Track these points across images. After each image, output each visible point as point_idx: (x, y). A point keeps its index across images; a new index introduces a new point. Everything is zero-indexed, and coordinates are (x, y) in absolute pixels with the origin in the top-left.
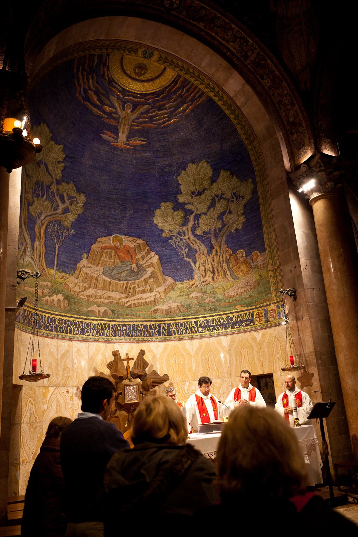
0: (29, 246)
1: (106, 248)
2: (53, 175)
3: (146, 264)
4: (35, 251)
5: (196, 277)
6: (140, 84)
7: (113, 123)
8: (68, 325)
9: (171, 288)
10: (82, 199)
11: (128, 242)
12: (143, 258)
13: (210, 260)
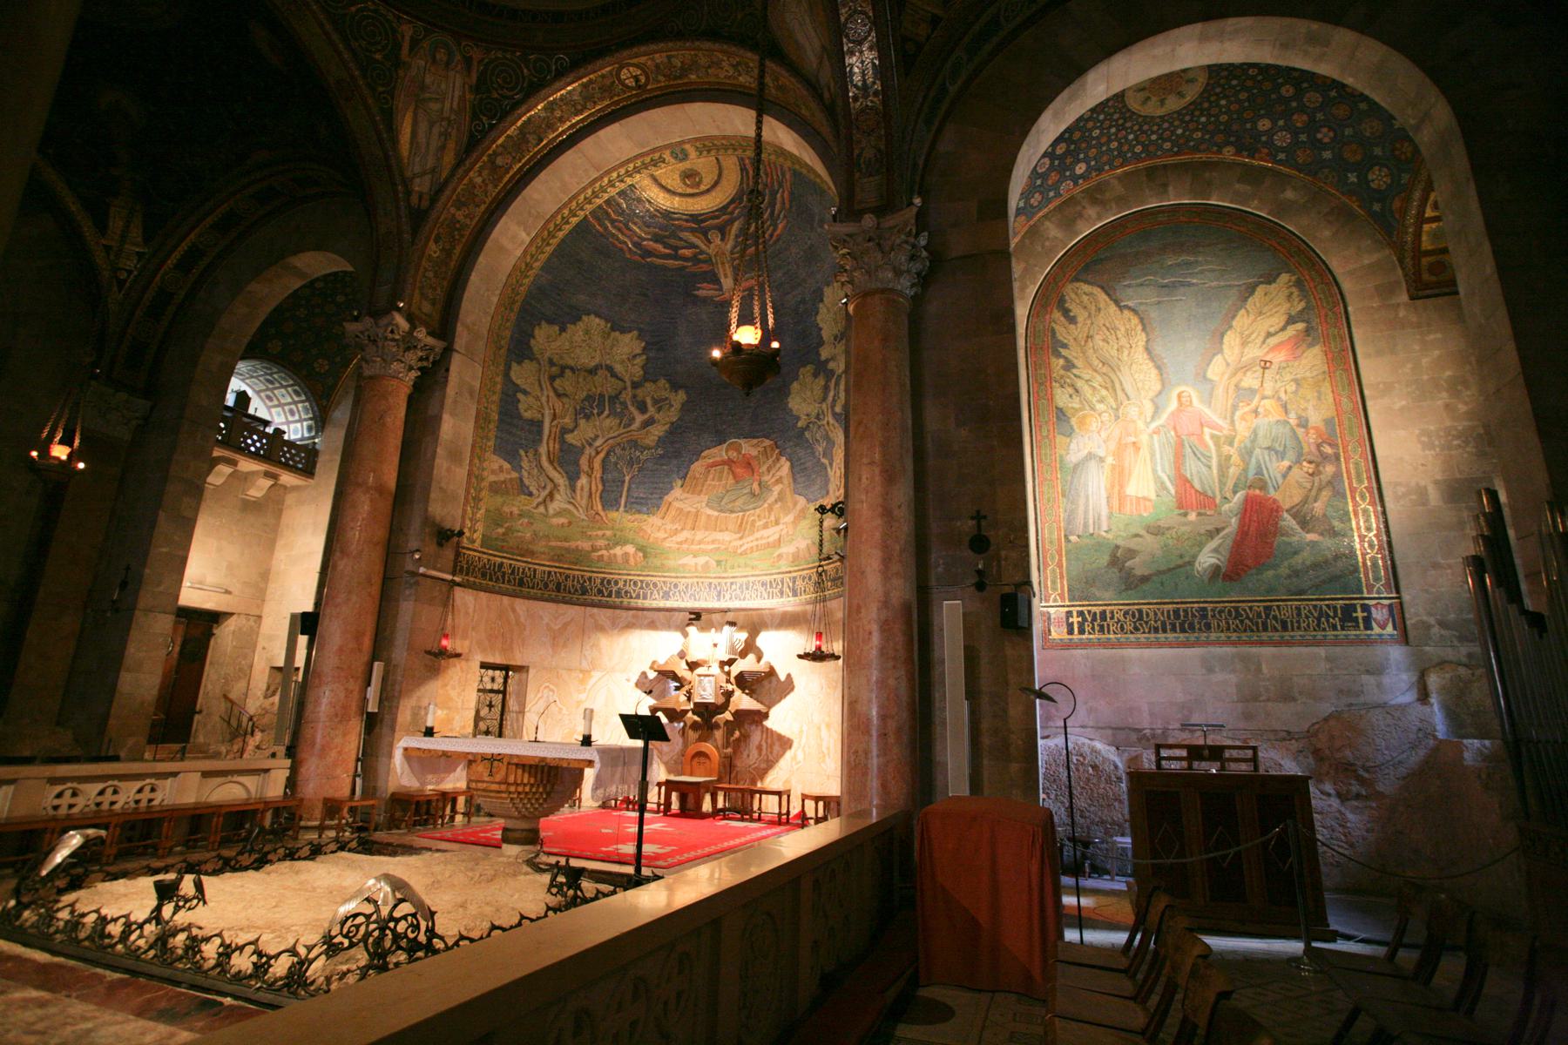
0: (562, 489)
2: (626, 379)
3: (773, 480)
4: (578, 492)
5: (831, 492)
6: (708, 197)
7: (705, 267)
8: (642, 588)
11: (748, 448)
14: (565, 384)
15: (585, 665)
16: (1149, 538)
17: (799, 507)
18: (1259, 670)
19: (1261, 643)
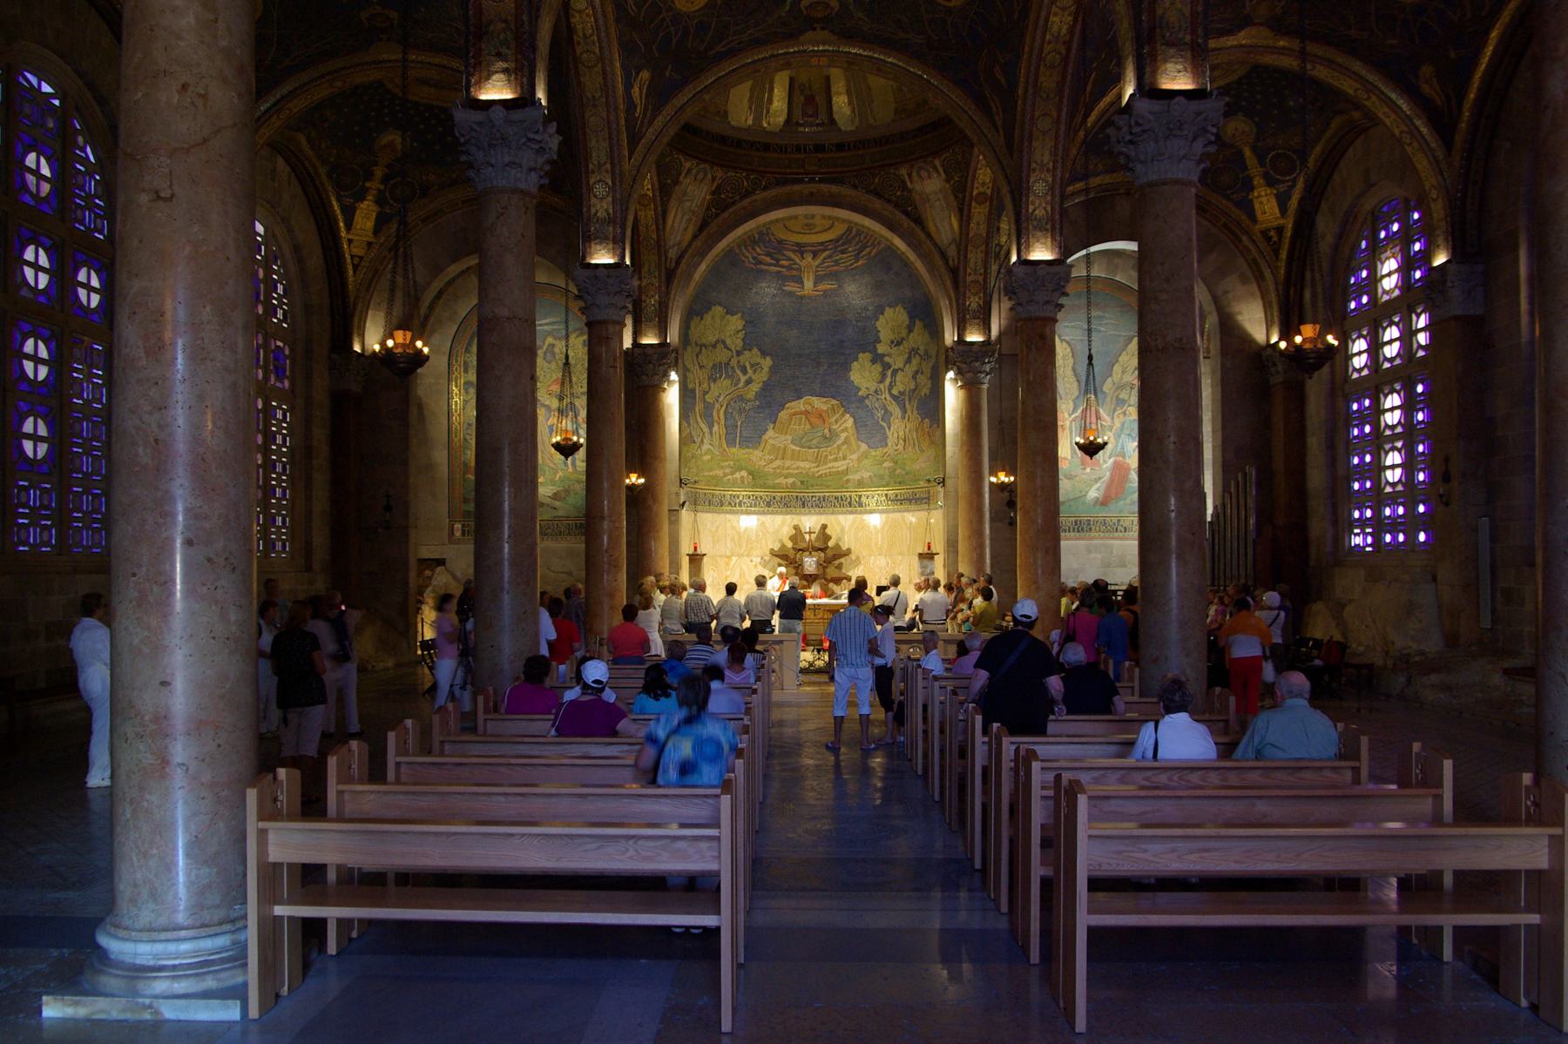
1: (795, 414)
5: (889, 444)
7: (795, 273)
9: (865, 456)
10: (767, 362)
11: (819, 403)
12: (836, 422)
13: (903, 427)
14: (703, 359)
15: (728, 553)
16: (1066, 481)
17: (861, 450)
18: (1112, 552)
19: (1114, 538)
